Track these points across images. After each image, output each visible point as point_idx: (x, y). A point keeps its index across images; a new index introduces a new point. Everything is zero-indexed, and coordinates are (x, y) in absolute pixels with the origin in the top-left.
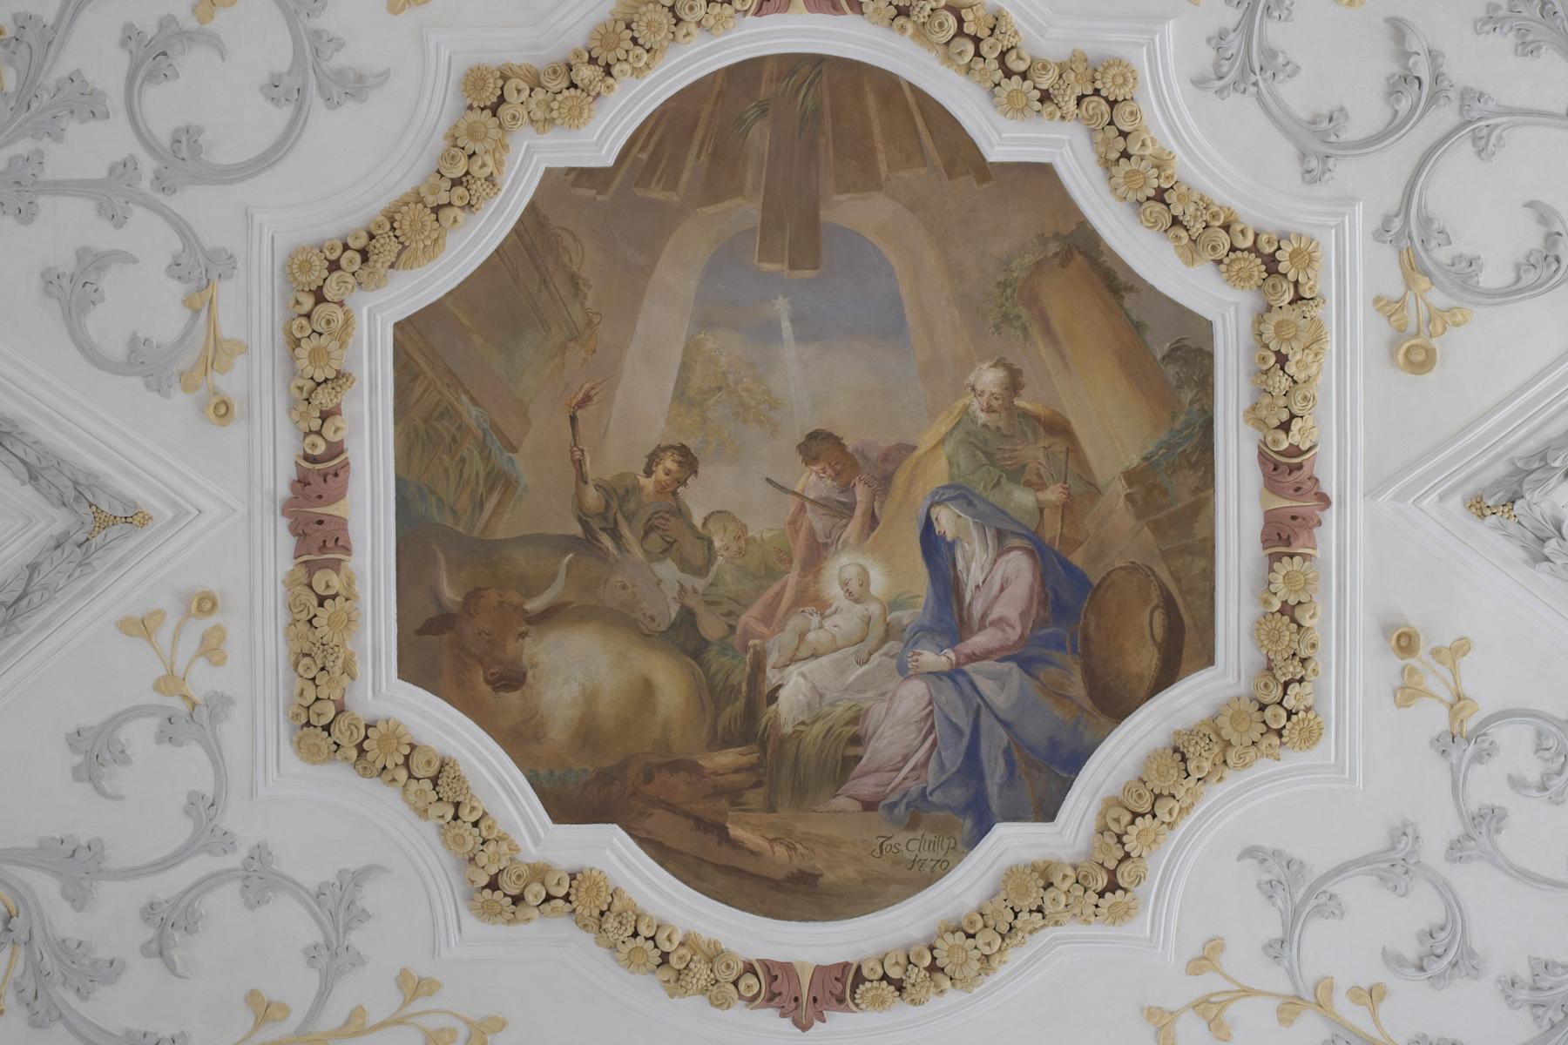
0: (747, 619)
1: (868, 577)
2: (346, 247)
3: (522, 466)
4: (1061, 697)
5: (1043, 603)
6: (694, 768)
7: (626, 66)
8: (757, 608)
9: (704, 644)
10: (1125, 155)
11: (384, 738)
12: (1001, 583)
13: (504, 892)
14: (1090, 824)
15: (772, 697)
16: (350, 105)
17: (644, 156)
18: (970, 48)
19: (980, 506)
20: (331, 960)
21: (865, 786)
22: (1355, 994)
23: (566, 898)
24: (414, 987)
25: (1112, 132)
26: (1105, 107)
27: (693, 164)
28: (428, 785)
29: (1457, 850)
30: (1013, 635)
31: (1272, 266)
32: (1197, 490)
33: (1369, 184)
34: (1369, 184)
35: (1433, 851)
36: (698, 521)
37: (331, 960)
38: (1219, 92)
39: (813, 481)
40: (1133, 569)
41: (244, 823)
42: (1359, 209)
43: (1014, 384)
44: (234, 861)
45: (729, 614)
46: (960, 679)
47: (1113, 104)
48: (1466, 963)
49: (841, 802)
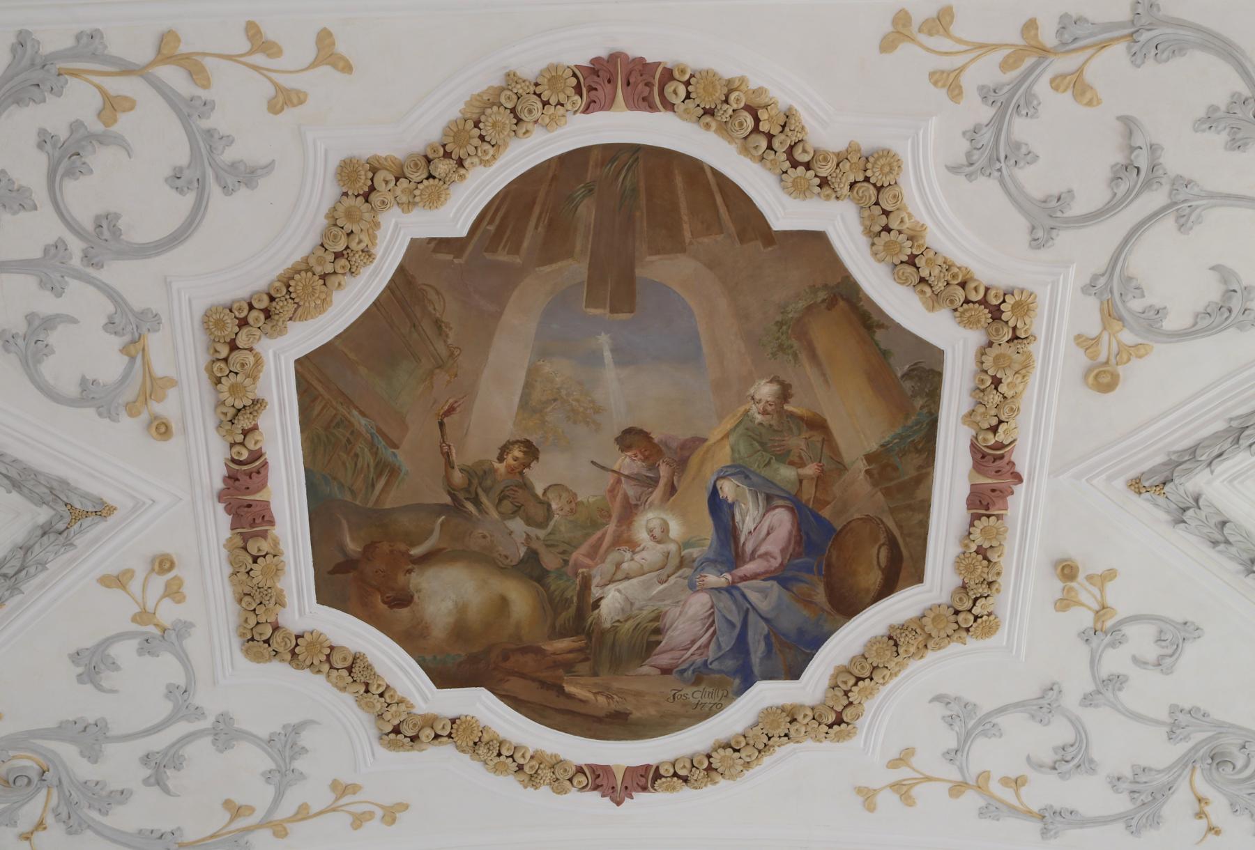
0: (578, 555)
1: (667, 527)
2: (251, 307)
3: (402, 458)
4: (807, 602)
5: (798, 543)
6: (538, 651)
7: (476, 160)
8: (584, 548)
9: (546, 572)
10: (887, 229)
11: (311, 645)
12: (767, 529)
13: (404, 732)
14: (825, 683)
15: (596, 605)
16: (243, 191)
17: (492, 228)
18: (764, 144)
19: (755, 479)
20: (282, 777)
21: (664, 660)
22: (1005, 781)
23: (450, 736)
24: (342, 789)
25: (877, 210)
26: (873, 191)
27: (532, 235)
28: (345, 673)
29: (1088, 700)
30: (775, 563)
31: (998, 314)
32: (920, 467)
33: (1084, 251)
34: (1084, 251)
35: (1071, 700)
36: (539, 491)
37: (282, 777)
38: (969, 176)
39: (628, 463)
40: (867, 519)
41: (210, 700)
42: (1073, 270)
43: (785, 394)
44: (206, 724)
45: (564, 552)
46: (735, 592)
47: (879, 189)
48: (1087, 765)
49: (645, 669)
